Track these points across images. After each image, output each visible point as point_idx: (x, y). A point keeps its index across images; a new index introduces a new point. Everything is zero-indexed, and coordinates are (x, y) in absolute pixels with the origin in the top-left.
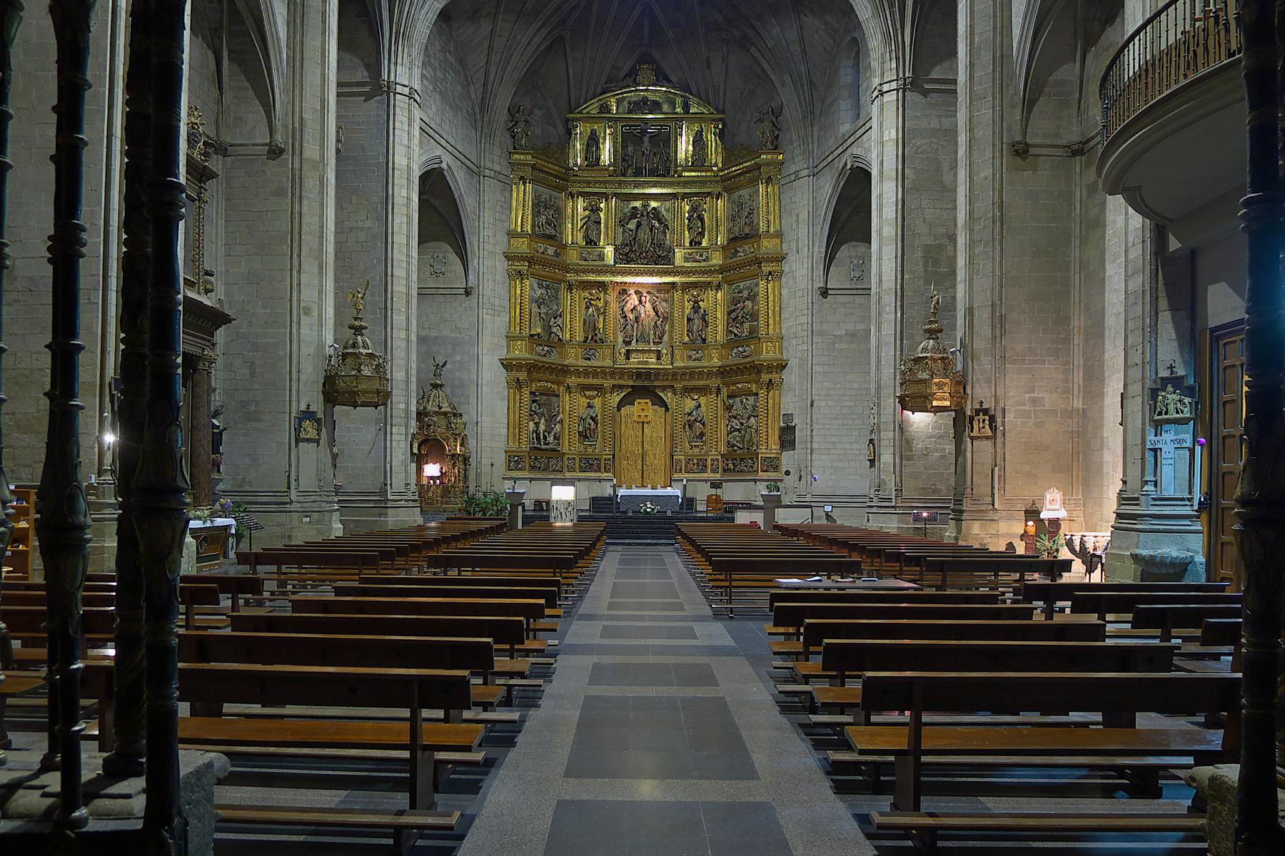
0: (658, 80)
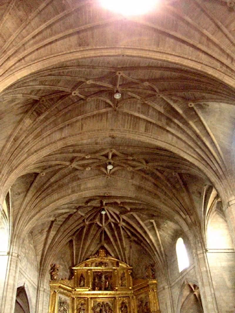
0: (107, 255)
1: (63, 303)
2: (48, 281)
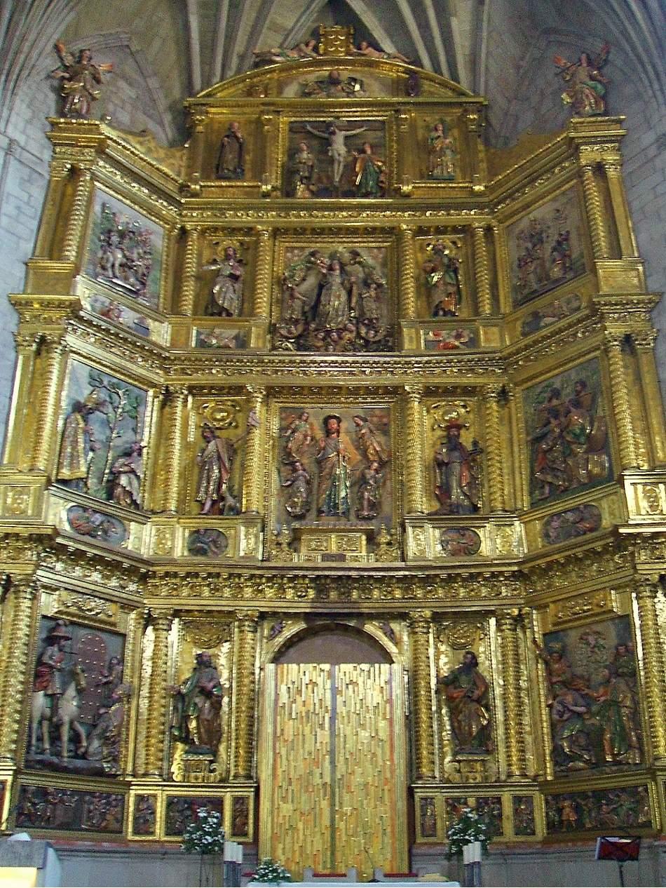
1: (122, 235)
2: (42, 116)
